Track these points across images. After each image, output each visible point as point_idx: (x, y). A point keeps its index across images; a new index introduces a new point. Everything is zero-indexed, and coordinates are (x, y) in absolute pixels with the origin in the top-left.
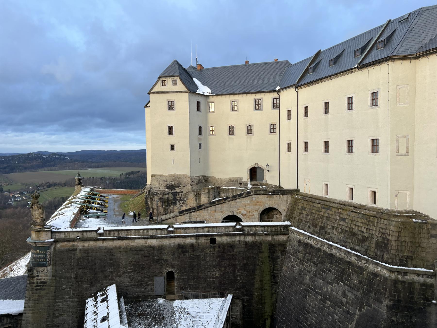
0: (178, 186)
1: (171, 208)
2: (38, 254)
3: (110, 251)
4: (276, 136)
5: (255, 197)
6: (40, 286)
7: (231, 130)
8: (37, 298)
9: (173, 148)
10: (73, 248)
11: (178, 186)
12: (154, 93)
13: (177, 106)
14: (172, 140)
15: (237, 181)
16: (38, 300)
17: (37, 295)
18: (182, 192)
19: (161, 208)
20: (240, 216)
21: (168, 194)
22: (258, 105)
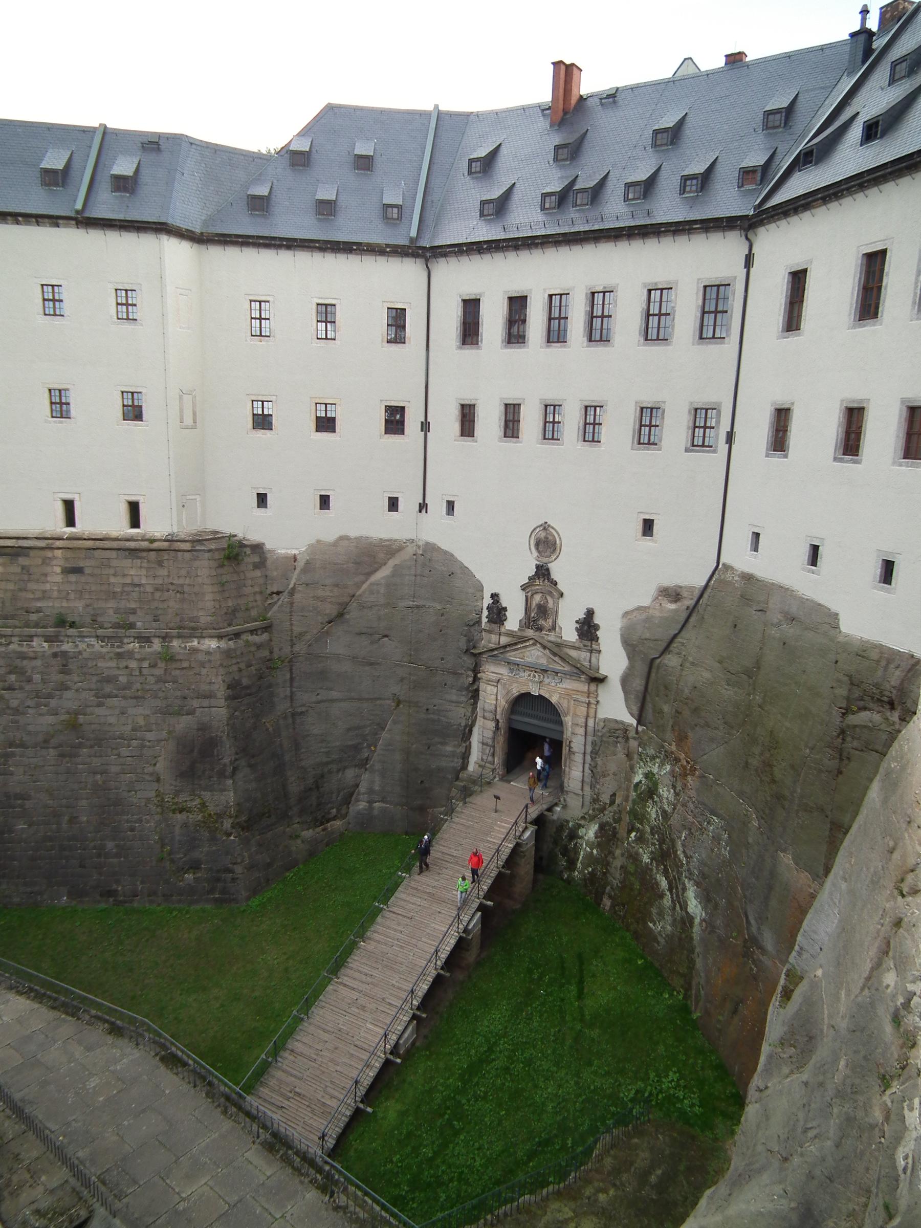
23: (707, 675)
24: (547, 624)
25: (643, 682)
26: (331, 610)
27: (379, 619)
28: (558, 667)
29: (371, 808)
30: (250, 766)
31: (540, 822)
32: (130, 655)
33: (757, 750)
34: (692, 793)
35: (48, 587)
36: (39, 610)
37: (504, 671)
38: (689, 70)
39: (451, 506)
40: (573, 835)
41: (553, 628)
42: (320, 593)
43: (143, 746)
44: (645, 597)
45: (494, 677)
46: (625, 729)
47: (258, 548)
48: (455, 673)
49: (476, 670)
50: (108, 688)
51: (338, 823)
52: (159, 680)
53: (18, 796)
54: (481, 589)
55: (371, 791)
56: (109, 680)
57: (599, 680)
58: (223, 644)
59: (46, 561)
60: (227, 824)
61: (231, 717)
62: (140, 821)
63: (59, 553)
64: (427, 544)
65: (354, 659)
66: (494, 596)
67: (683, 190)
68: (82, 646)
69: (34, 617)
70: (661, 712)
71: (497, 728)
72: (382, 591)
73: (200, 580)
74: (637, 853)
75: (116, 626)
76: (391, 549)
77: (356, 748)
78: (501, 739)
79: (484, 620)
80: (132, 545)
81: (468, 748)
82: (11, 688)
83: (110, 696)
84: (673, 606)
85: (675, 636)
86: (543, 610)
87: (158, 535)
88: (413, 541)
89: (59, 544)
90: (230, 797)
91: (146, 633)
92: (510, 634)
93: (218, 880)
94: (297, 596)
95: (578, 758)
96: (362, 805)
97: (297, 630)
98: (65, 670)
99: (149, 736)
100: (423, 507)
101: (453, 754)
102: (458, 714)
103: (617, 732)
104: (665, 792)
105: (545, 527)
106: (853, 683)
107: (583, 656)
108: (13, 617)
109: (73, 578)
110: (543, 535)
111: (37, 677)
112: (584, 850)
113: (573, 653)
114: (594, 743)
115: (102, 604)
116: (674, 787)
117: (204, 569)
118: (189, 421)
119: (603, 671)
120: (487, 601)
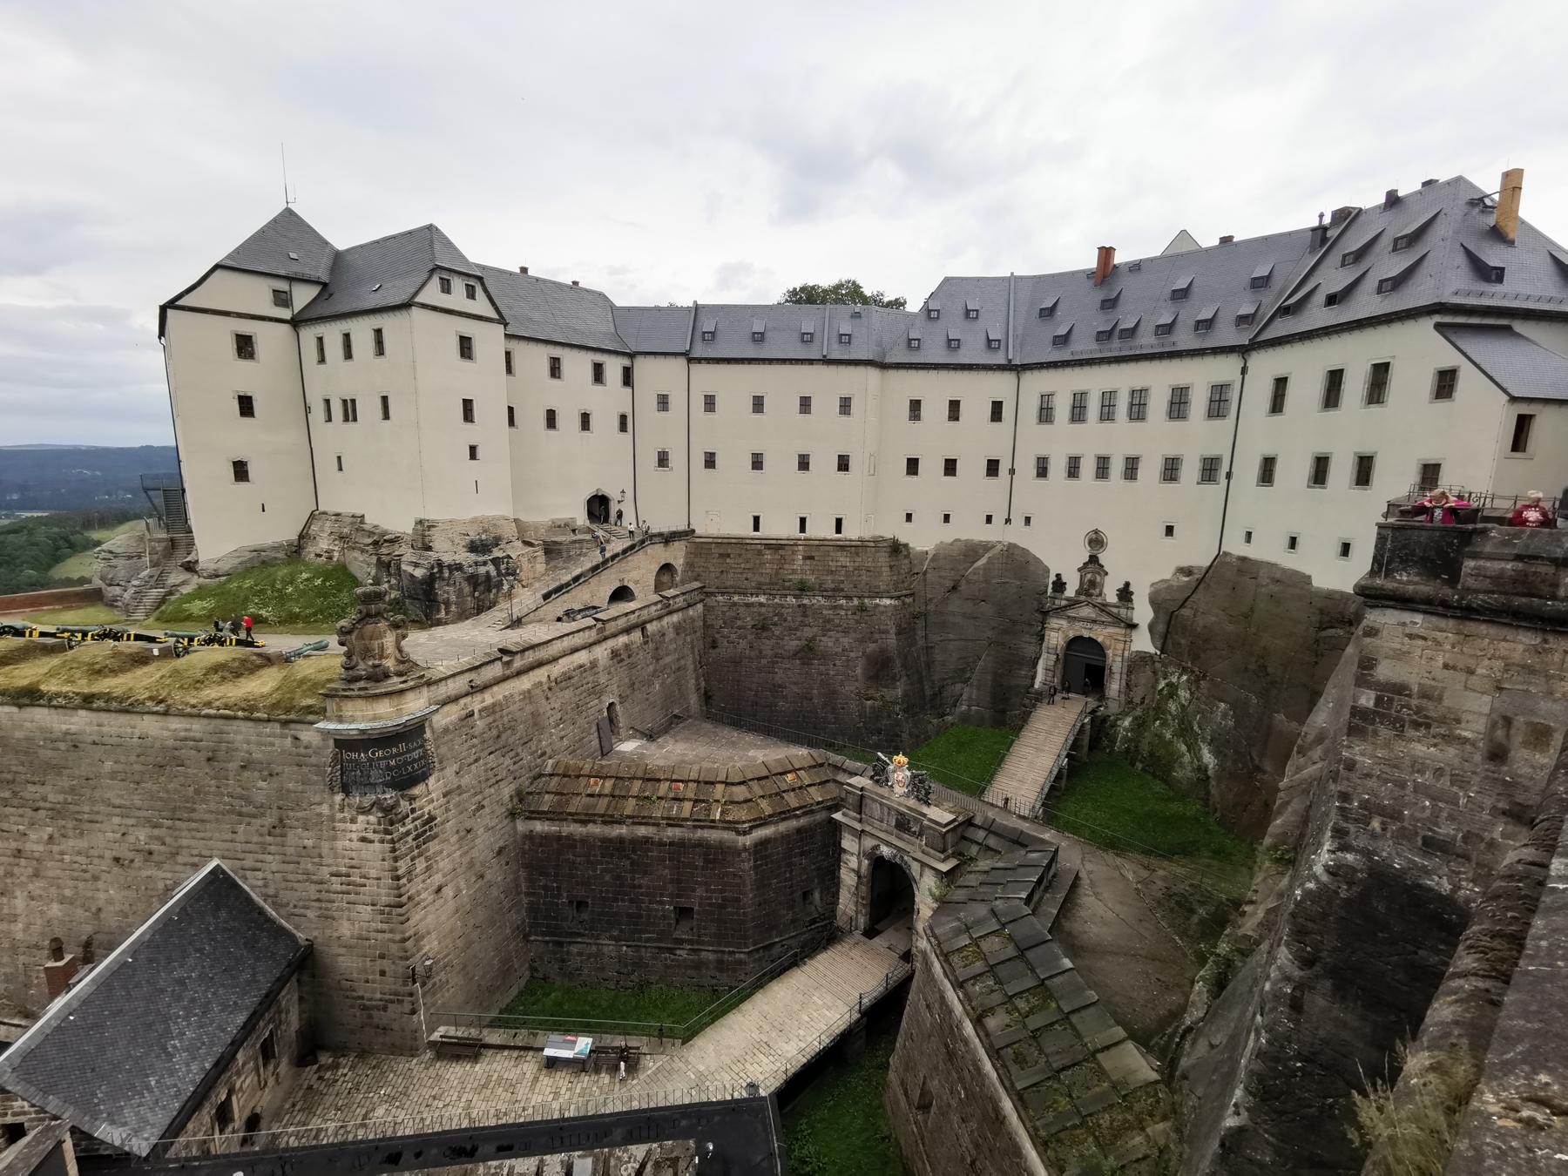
0: (497, 541)
1: (492, 596)
2: (404, 753)
3: (528, 695)
4: (628, 436)
5: (650, 550)
6: (425, 831)
7: (551, 419)
8: (425, 865)
9: (473, 451)
10: (464, 713)
11: (497, 541)
12: (424, 306)
13: (478, 348)
14: (471, 433)
15: (566, 525)
16: (428, 868)
17: (422, 859)
18: (509, 557)
19: (469, 599)
20: (631, 585)
21: (485, 563)
22: (598, 373)
23: (1213, 619)
24: (1098, 591)
25: (1165, 627)
26: (949, 584)
27: (979, 590)
28: (1103, 619)
29: (969, 710)
30: (908, 676)
31: (1093, 712)
32: (841, 607)
33: (1254, 659)
34: (1205, 691)
35: (795, 567)
36: (790, 580)
37: (1064, 623)
38: (1185, 248)
39: (1028, 520)
40: (1114, 725)
41: (1100, 594)
42: (943, 574)
43: (848, 661)
44: (1167, 574)
45: (1057, 626)
46: (1151, 656)
47: (906, 546)
48: (1030, 625)
49: (1043, 623)
50: (828, 626)
51: (950, 718)
52: (857, 622)
53: (780, 686)
54: (1047, 571)
55: (970, 699)
56: (829, 621)
57: (1134, 626)
58: (893, 602)
59: (794, 553)
60: (897, 708)
61: (898, 645)
62: (847, 703)
63: (801, 548)
64: (1010, 544)
65: (964, 615)
66: (1058, 576)
67: (1197, 329)
68: (814, 601)
69: (787, 584)
70: (1179, 644)
71: (1058, 659)
72: (981, 572)
73: (879, 564)
74: (1162, 733)
75: (834, 590)
76: (987, 547)
77: (963, 671)
78: (1060, 666)
79: (1050, 590)
80: (841, 543)
81: (1036, 673)
82: (775, 624)
83: (829, 630)
84: (1187, 579)
85: (1189, 597)
86: (1093, 584)
87: (853, 538)
88: (1000, 542)
89: (800, 542)
90: (899, 692)
91: (849, 594)
92: (1068, 599)
93: (892, 741)
94: (929, 576)
95: (1117, 676)
96: (964, 708)
97: (929, 596)
98: (805, 615)
99: (852, 655)
100: (1008, 521)
101: (1026, 676)
102: (1029, 650)
103: (1142, 659)
104: (1184, 694)
105: (1096, 532)
106: (1322, 612)
107: (1123, 611)
108: (776, 584)
109: (808, 562)
110: (1094, 536)
111: (789, 618)
112: (1122, 733)
113: (1115, 610)
114: (1129, 666)
115: (825, 577)
116: (1190, 690)
117: (883, 559)
118: (872, 472)
119: (1135, 621)
120: (1052, 578)
